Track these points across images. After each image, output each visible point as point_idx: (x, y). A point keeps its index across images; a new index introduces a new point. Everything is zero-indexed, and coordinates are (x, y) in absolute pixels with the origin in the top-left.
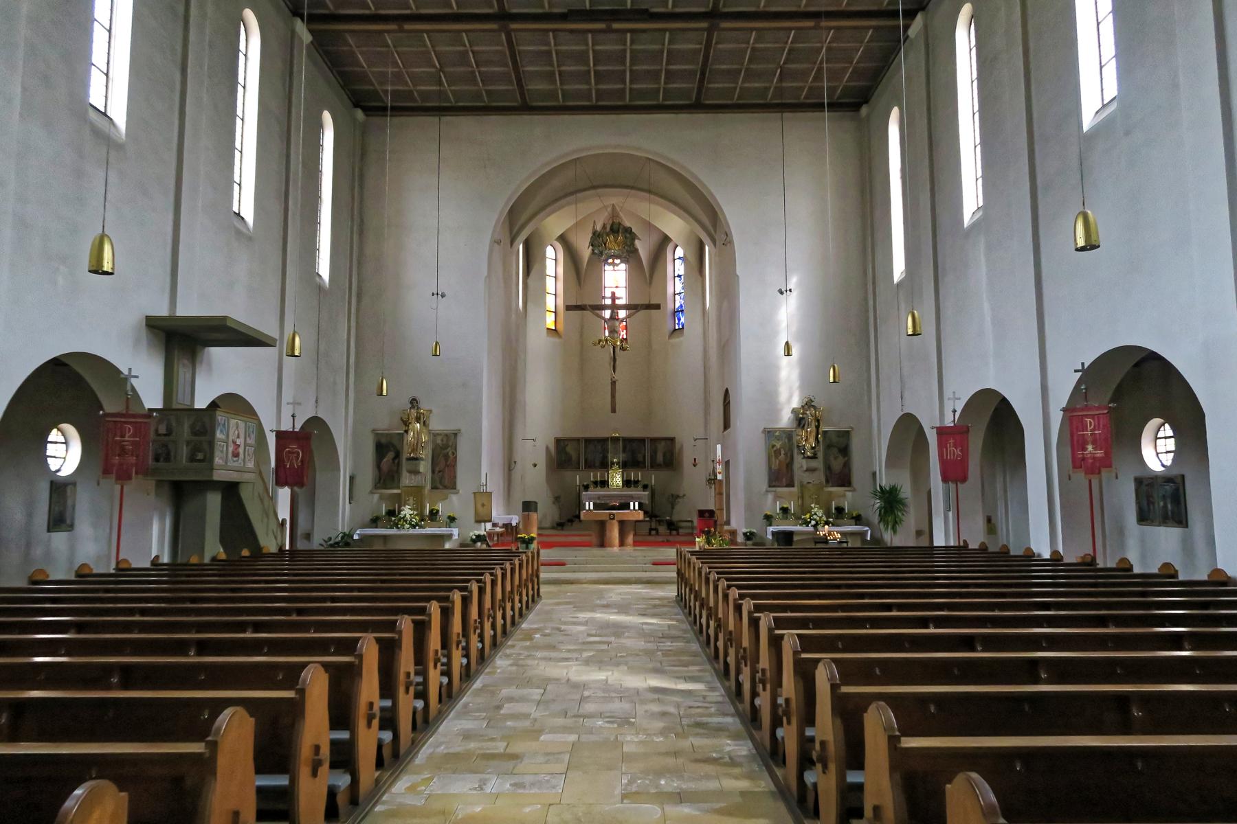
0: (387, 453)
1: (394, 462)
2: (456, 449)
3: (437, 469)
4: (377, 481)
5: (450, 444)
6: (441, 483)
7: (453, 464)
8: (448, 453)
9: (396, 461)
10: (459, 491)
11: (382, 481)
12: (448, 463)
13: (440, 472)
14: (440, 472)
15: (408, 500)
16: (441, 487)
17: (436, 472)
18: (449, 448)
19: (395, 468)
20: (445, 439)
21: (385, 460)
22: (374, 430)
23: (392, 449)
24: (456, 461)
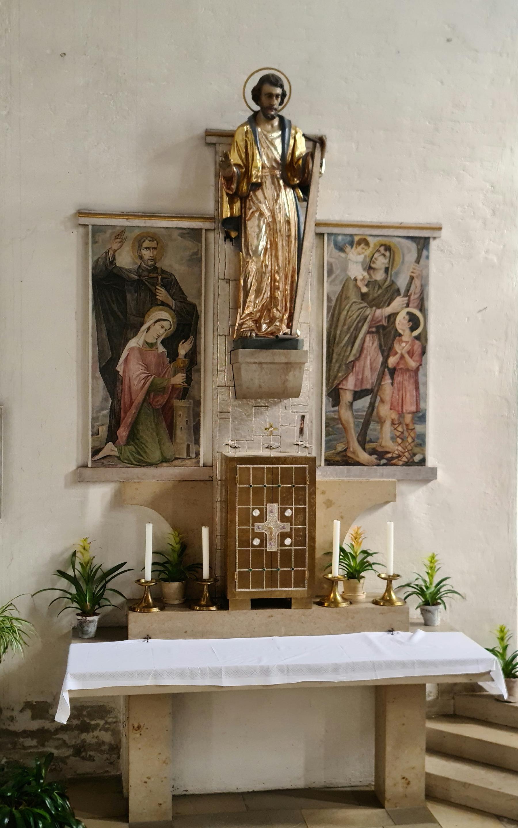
0: (142, 316)
1: (173, 355)
2: (422, 308)
3: (350, 384)
4: (103, 431)
5: (402, 283)
6: (363, 442)
7: (412, 364)
8: (391, 318)
9: (183, 349)
10: (434, 470)
11: (123, 433)
12: (392, 361)
13: (358, 395)
14: (358, 395)
15: (262, 518)
16: (363, 456)
17: (347, 397)
18: (398, 302)
19: (179, 379)
20: (381, 262)
21: (133, 343)
22: (81, 213)
23: (162, 294)
24: (424, 352)
